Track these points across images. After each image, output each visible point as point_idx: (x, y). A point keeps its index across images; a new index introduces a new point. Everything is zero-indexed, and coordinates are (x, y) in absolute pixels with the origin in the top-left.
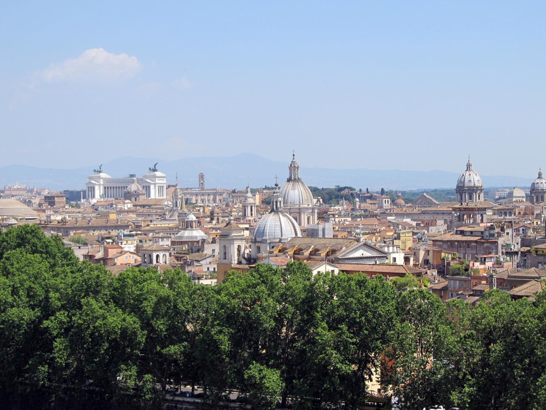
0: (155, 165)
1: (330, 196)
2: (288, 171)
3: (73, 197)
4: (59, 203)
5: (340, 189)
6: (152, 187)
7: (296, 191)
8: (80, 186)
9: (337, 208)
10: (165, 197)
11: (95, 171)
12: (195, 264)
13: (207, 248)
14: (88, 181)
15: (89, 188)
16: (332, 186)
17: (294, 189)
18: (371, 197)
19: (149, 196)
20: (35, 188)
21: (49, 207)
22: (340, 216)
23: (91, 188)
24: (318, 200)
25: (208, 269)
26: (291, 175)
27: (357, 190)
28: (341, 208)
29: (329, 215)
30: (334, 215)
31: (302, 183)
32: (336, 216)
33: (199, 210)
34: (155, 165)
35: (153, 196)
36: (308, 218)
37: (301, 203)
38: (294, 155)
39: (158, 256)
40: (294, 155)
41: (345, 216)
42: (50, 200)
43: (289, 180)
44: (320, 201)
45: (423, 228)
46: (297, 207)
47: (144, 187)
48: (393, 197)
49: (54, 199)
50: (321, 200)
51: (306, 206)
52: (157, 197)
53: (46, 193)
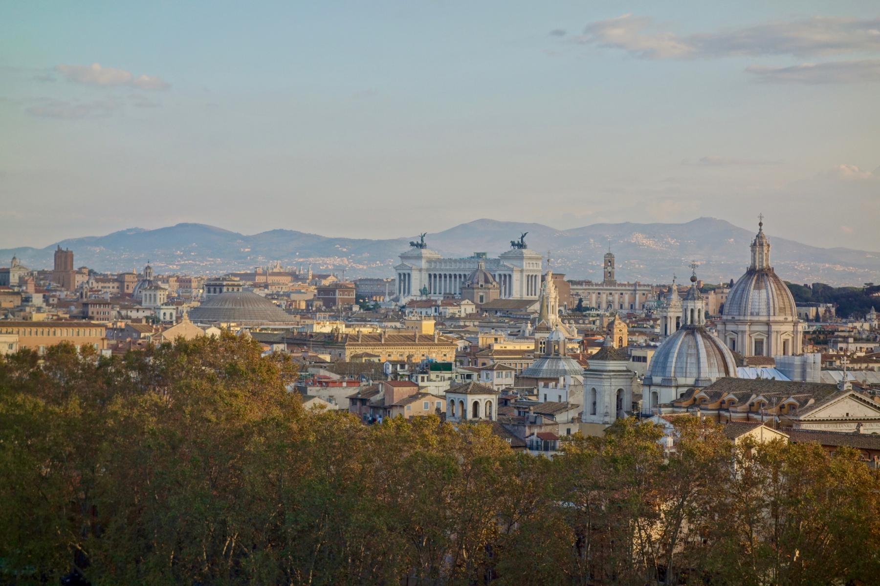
0: (523, 237)
1: (852, 303)
4: (343, 300)
6: (516, 276)
7: (764, 291)
9: (858, 325)
11: (412, 244)
12: (545, 420)
14: (399, 262)
15: (400, 275)
16: (859, 284)
19: (510, 294)
20: (311, 273)
21: (324, 308)
22: (856, 340)
25: (569, 431)
26: (755, 261)
28: (866, 326)
29: (838, 337)
31: (775, 276)
32: (851, 340)
33: (594, 322)
34: (523, 237)
36: (784, 343)
37: (772, 314)
38: (760, 224)
39: (476, 404)
40: (760, 224)
41: (868, 340)
43: (751, 272)
44: (830, 311)
46: (765, 319)
47: (500, 275)
49: (334, 295)
50: (833, 310)
51: (781, 318)
52: (525, 297)
53: (326, 283)
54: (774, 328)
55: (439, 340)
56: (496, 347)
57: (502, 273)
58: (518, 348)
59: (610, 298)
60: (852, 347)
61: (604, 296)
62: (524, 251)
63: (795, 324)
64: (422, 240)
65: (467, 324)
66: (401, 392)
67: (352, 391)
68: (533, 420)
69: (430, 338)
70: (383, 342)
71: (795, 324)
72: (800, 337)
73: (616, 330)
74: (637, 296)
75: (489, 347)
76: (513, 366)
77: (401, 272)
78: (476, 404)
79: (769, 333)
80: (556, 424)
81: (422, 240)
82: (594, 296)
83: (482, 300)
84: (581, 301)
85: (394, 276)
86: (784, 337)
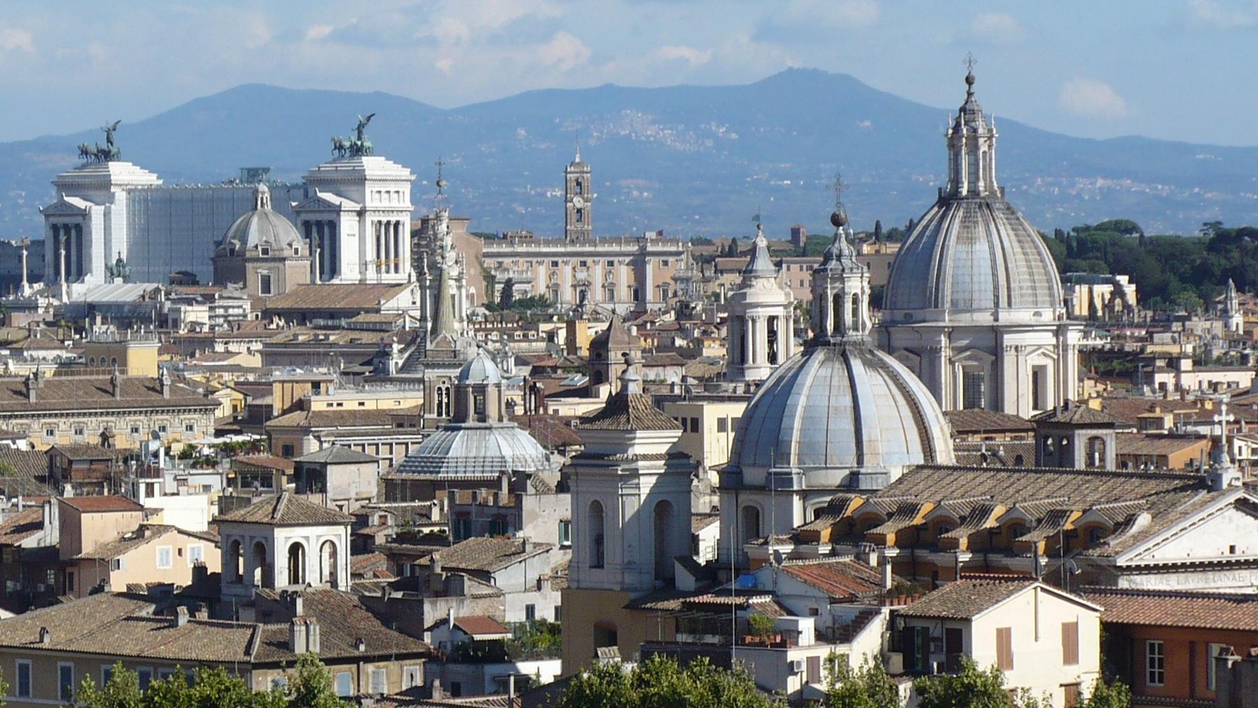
2: (944, 153)
5: (1222, 240)
6: (348, 225)
7: (981, 247)
10: (401, 277)
11: (84, 152)
12: (470, 586)
13: (535, 516)
14: (52, 198)
15: (55, 228)
17: (971, 241)
22: (1200, 362)
23: (67, 228)
24: (1118, 292)
25: (530, 610)
30: (1173, 364)
32: (1186, 364)
33: (551, 336)
34: (360, 127)
35: (349, 272)
36: (1035, 374)
38: (969, 81)
39: (295, 549)
40: (969, 81)
41: (1224, 363)
43: (947, 200)
46: (985, 319)
50: (1130, 291)
52: (371, 276)
54: (1009, 340)
55: (173, 389)
56: (318, 405)
57: (313, 217)
58: (370, 405)
59: (582, 275)
61: (568, 270)
62: (366, 160)
63: (1059, 331)
64: (109, 141)
65: (233, 347)
66: (98, 528)
68: (440, 587)
69: (155, 387)
70: (33, 399)
71: (1059, 331)
72: (1073, 359)
73: (615, 356)
74: (649, 269)
75: (301, 405)
76: (370, 451)
77: (59, 221)
78: (295, 549)
79: (997, 352)
80: (499, 594)
81: (109, 141)
82: (542, 271)
83: (266, 286)
84: (509, 284)
85: (42, 231)
86: (1036, 360)
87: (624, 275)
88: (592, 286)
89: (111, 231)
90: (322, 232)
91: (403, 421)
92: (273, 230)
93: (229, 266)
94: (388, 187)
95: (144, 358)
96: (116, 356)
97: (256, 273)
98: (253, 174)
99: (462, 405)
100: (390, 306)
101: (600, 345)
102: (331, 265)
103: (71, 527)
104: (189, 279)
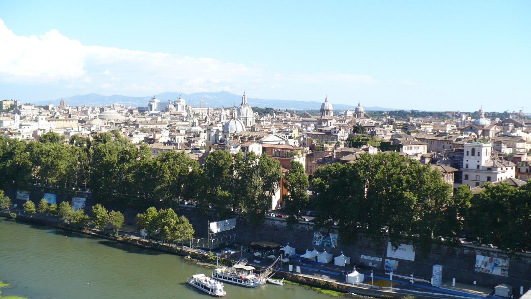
3: (142, 111)
5: (267, 109)
8: (146, 105)
14: (148, 103)
16: (263, 107)
18: (281, 113)
22: (266, 121)
27: (275, 109)
35: (179, 111)
42: (131, 111)
43: (242, 104)
45: (304, 128)
48: (292, 113)
53: (129, 108)
56: (177, 124)
60: (265, 123)
67: (145, 136)
79: (246, 119)
87: (207, 111)
88: (204, 113)
89: (155, 106)
90: (176, 106)
91: (186, 126)
92: (171, 106)
93: (167, 110)
94: (183, 102)
95: (159, 119)
96: (157, 119)
97: (170, 110)
98: (169, 100)
99: (193, 124)
100: (183, 114)
101: (206, 118)
102: (177, 110)
103: (154, 136)
104: (163, 111)
